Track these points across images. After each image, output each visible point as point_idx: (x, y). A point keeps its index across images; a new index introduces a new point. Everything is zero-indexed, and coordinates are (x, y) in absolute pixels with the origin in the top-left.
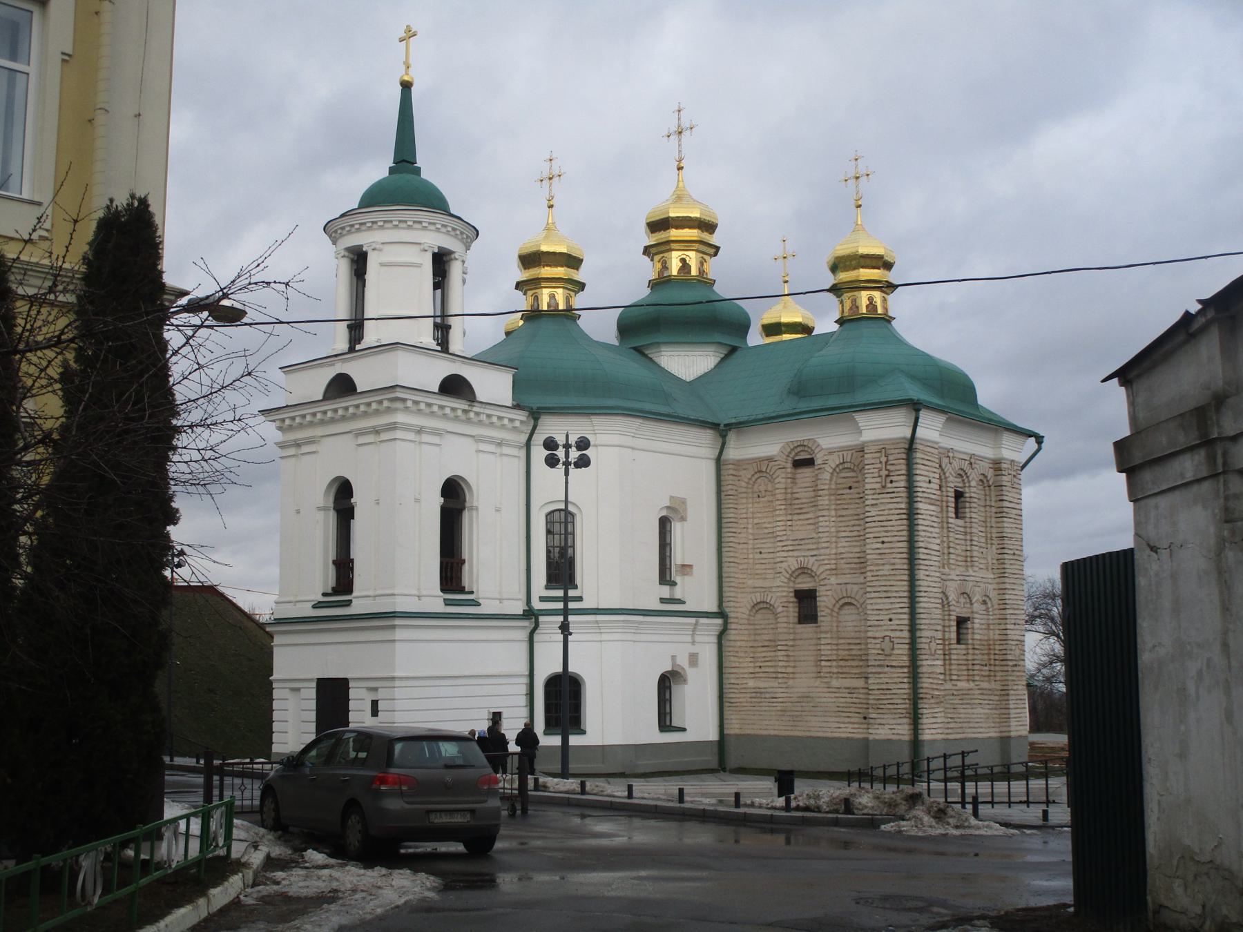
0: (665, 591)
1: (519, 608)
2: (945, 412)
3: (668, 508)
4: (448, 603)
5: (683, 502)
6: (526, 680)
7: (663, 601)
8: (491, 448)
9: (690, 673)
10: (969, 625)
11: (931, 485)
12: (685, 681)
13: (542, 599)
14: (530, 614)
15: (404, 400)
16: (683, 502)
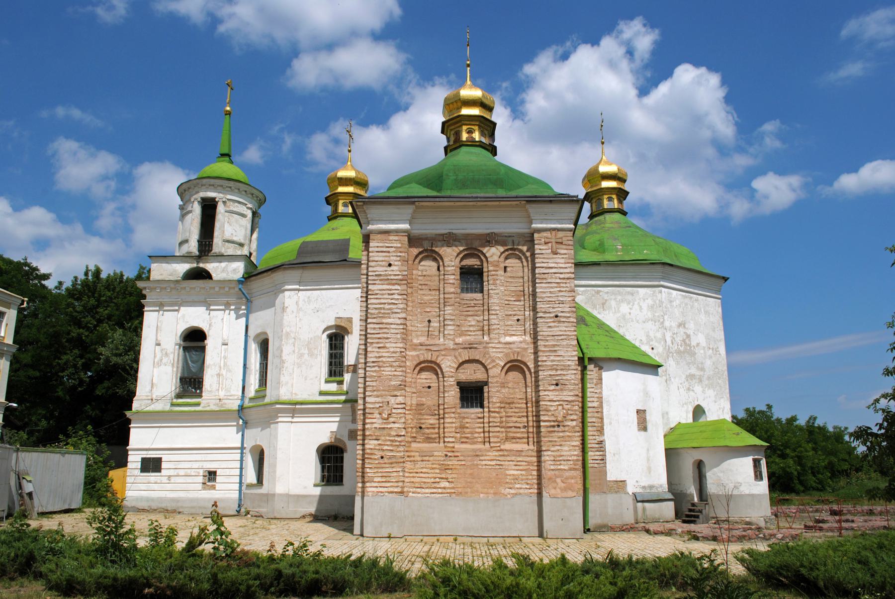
0: (333, 387)
1: (235, 405)
2: (413, 203)
3: (337, 327)
4: (172, 405)
5: (350, 320)
6: (239, 451)
7: (322, 393)
8: (223, 307)
9: (349, 444)
10: (486, 389)
11: (392, 268)
12: (346, 451)
13: (251, 399)
14: (242, 408)
15: (145, 288)
16: (350, 320)
